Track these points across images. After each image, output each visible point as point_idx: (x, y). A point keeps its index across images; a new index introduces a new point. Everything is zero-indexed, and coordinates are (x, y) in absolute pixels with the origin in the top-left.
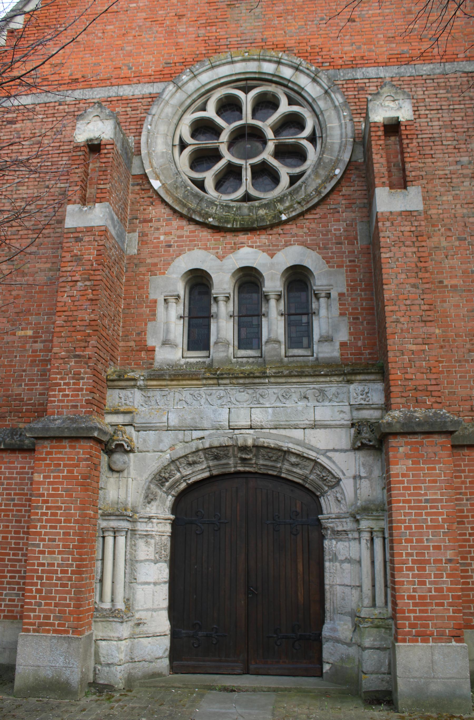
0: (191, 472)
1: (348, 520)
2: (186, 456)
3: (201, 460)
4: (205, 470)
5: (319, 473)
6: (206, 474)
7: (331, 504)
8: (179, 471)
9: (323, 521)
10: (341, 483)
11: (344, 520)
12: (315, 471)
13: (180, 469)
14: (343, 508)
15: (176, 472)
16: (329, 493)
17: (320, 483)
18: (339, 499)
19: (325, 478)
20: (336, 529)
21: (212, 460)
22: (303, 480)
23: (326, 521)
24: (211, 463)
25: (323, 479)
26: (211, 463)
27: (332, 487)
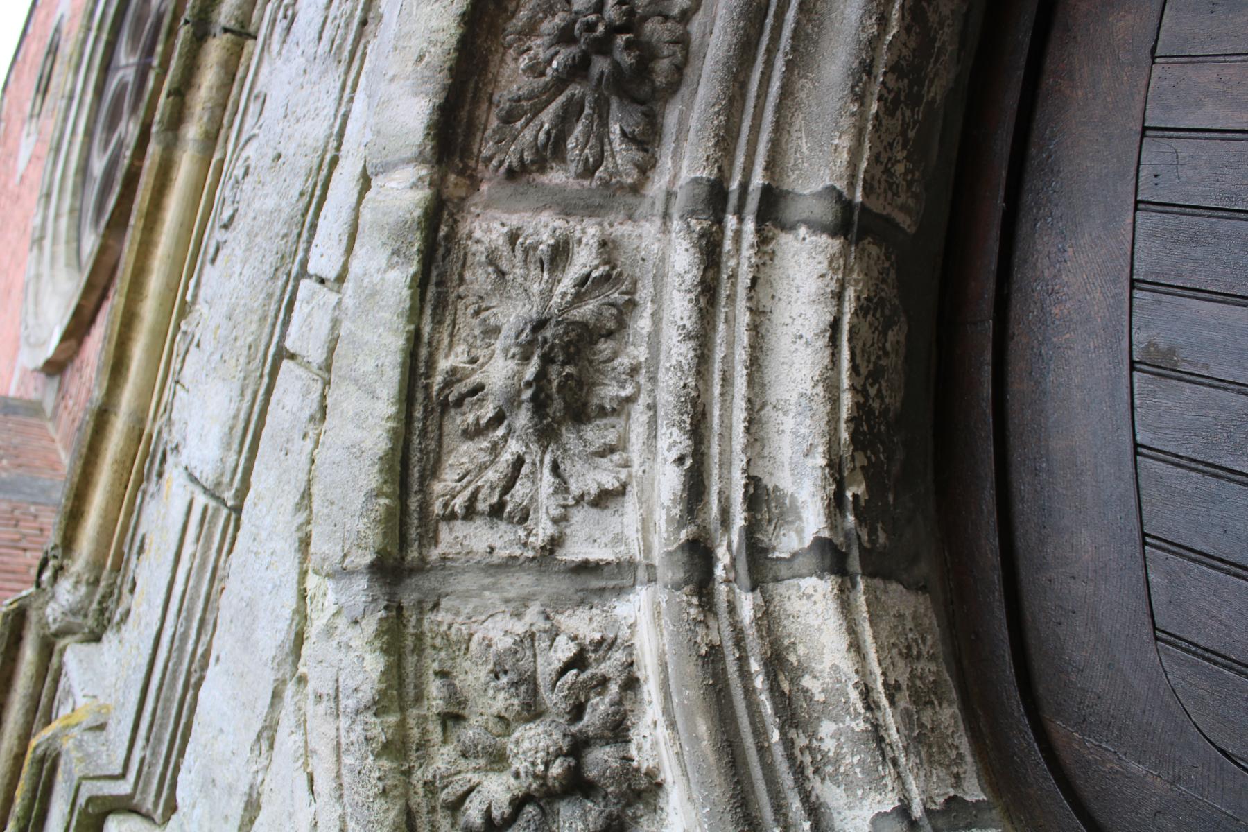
0: (673, 441)
2: (425, 406)
3: (583, 260)
4: (741, 260)
6: (806, 278)
8: (597, 580)
13: (575, 551)
15: (582, 624)
21: (646, 140)
24: (684, 164)
26: (684, 164)
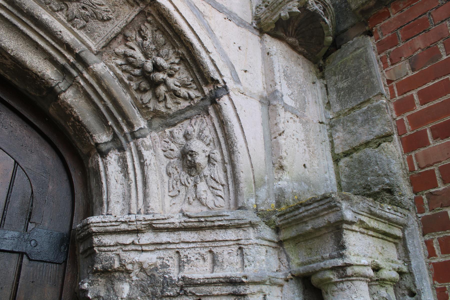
1: (251, 233)
5: (138, 54)
7: (153, 177)
9: (108, 240)
10: (224, 101)
11: (231, 235)
12: (121, 49)
14: (209, 198)
16: (148, 141)
17: (125, 99)
18: (201, 159)
19: (161, 76)
20: (174, 274)
22: (63, 70)
23: (127, 239)
25: (148, 81)
27: (167, 120)
